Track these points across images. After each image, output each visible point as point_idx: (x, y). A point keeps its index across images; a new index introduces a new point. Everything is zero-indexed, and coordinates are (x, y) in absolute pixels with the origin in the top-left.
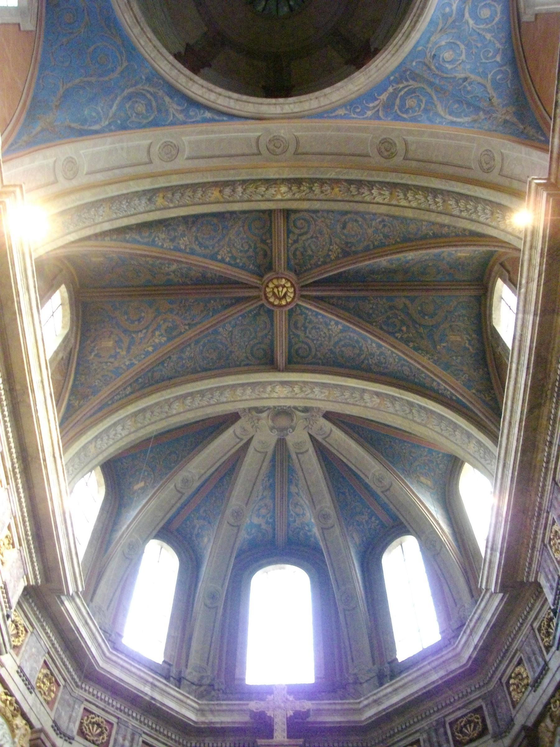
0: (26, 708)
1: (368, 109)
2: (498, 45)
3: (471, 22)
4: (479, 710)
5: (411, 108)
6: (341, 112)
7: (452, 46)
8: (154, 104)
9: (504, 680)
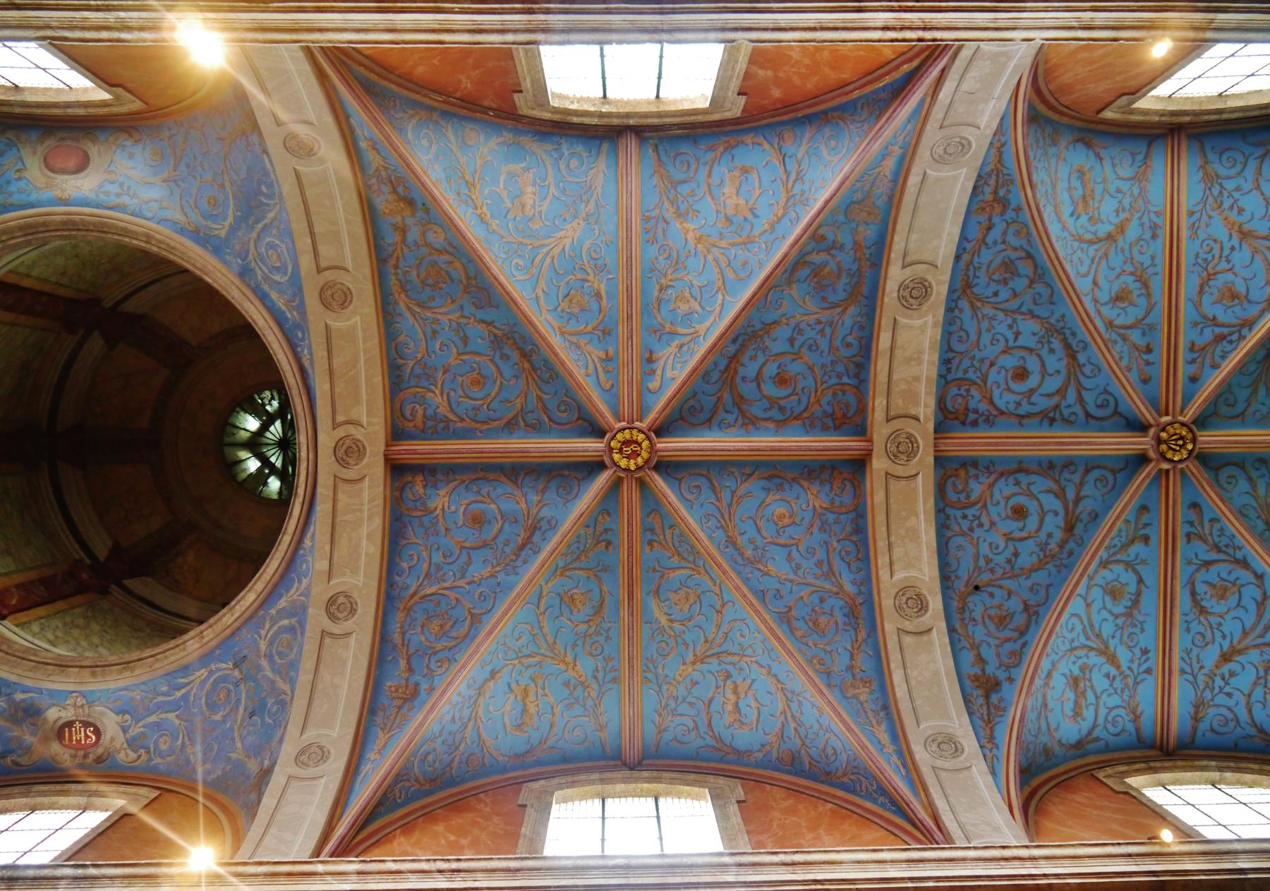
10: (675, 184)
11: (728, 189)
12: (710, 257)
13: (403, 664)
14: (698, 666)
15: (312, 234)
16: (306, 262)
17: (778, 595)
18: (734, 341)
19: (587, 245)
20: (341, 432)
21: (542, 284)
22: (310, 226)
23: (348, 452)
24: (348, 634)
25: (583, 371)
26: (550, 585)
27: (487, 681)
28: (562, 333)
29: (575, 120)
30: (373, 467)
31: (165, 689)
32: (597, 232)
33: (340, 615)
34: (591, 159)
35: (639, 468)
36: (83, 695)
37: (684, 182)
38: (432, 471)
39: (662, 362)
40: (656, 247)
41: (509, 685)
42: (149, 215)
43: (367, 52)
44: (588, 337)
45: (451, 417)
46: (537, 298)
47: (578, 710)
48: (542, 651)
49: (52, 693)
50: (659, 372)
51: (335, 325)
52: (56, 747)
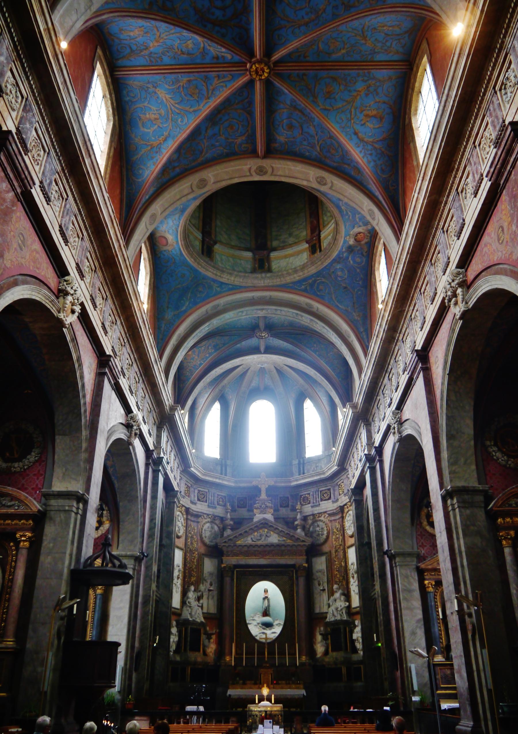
0: (184, 504)
1: (303, 285)
2: (361, 276)
3: (351, 262)
4: (329, 489)
5: (321, 290)
6: (291, 285)
7: (342, 270)
8: (206, 286)
9: (338, 484)
10: (132, 51)
11: (132, 34)
12: (165, 38)
13: (346, 166)
14: (368, 39)
15: (180, 198)
16: (190, 197)
17: (336, 7)
18: (205, 26)
19: (167, 86)
20: (254, 174)
21: (187, 108)
22: (178, 200)
23: (261, 171)
24: (332, 183)
25: (225, 89)
26: (320, 104)
27: (358, 137)
28: (208, 98)
29: (115, 104)
30: (267, 163)
31: (347, 217)
32: (160, 83)
33: (324, 182)
34: (129, 87)
35: (269, 68)
36: (345, 236)
37: (130, 48)
38: (270, 139)
39: (218, 53)
40: (163, 57)
41: (362, 125)
42: (178, 223)
43: (119, 216)
44: (208, 84)
45: (246, 135)
46: (194, 111)
47: (380, 90)
48: (350, 108)
49: (344, 243)
50: (223, 54)
51: (212, 181)
52: (363, 242)
